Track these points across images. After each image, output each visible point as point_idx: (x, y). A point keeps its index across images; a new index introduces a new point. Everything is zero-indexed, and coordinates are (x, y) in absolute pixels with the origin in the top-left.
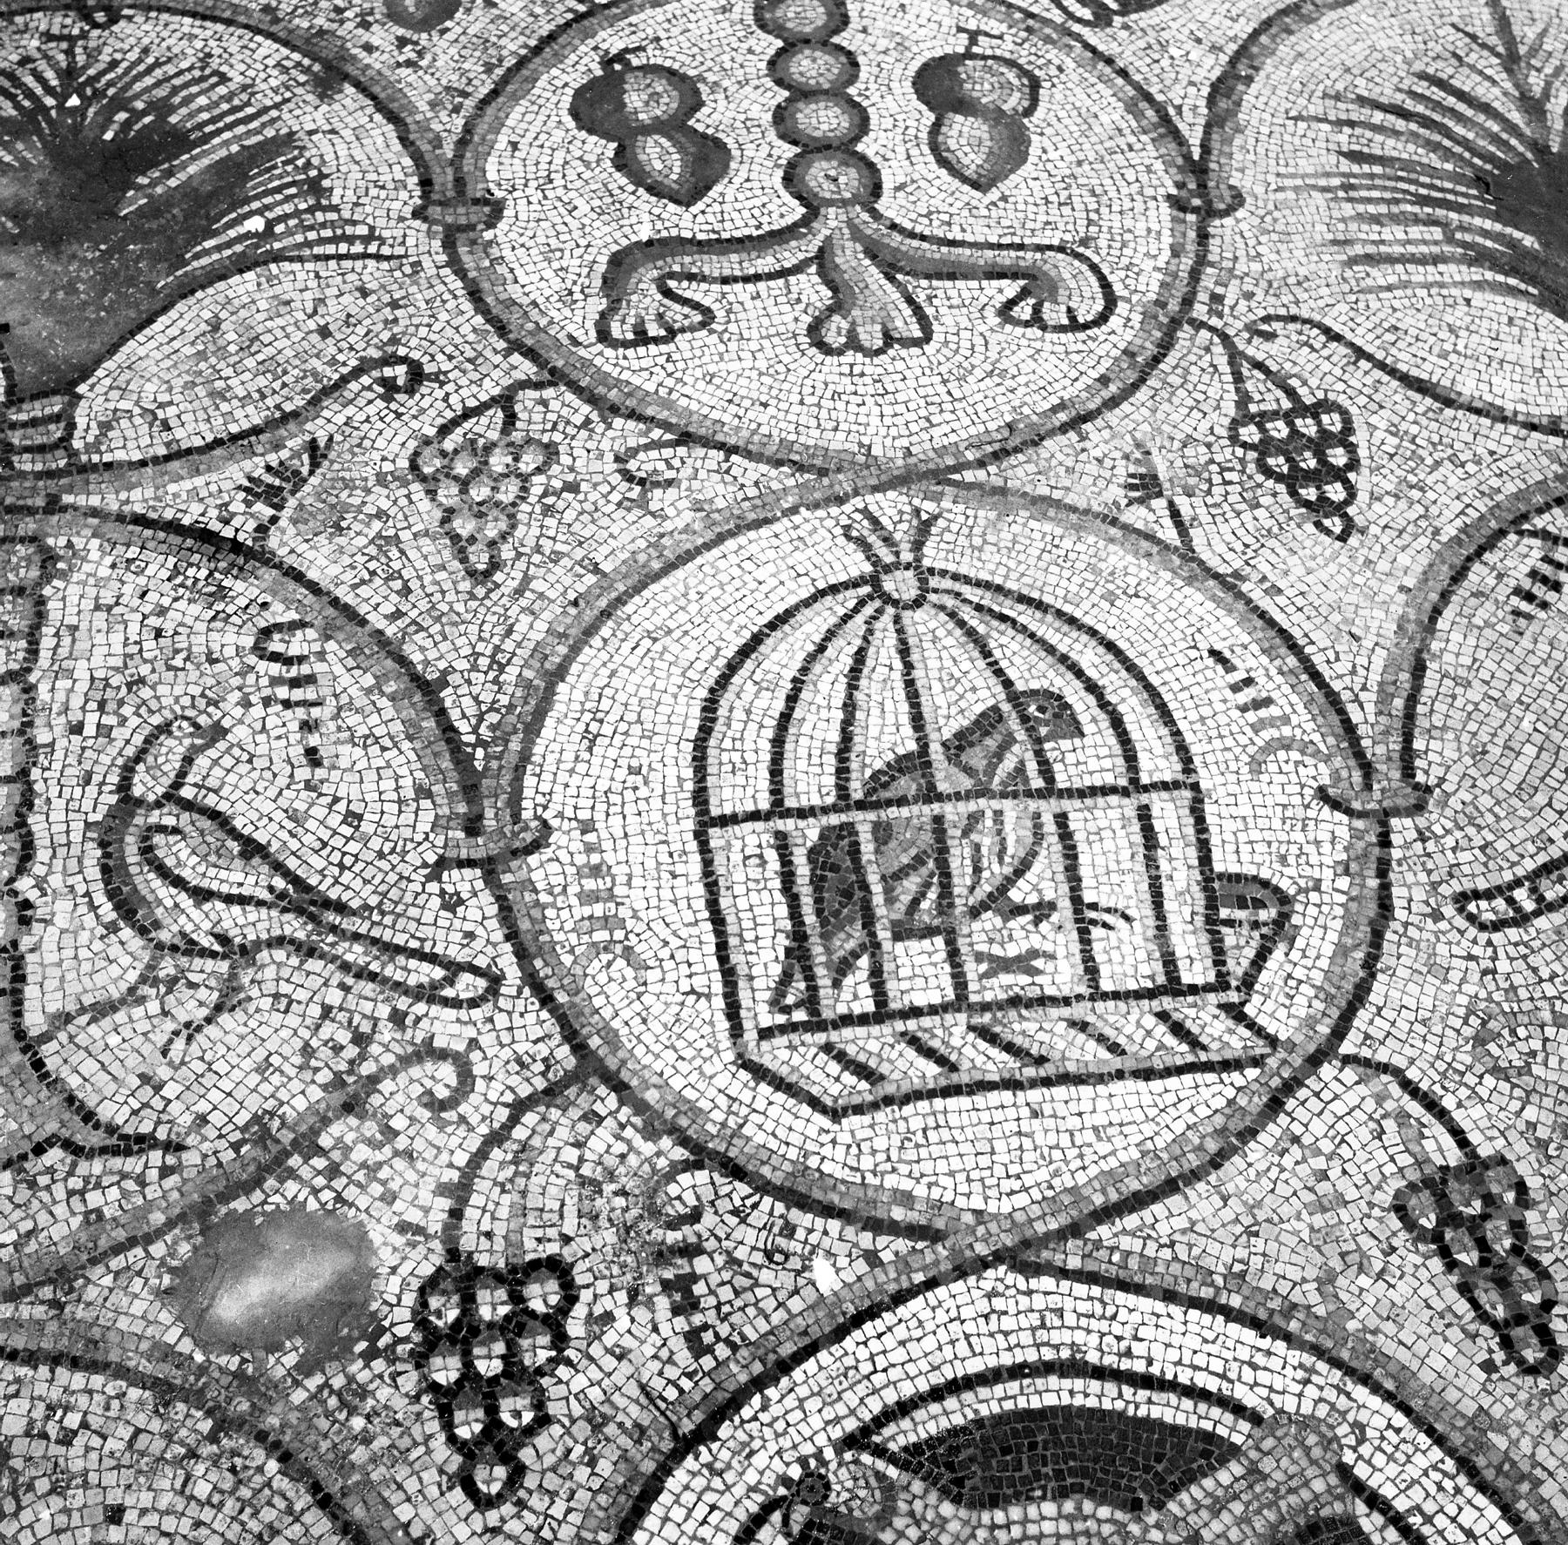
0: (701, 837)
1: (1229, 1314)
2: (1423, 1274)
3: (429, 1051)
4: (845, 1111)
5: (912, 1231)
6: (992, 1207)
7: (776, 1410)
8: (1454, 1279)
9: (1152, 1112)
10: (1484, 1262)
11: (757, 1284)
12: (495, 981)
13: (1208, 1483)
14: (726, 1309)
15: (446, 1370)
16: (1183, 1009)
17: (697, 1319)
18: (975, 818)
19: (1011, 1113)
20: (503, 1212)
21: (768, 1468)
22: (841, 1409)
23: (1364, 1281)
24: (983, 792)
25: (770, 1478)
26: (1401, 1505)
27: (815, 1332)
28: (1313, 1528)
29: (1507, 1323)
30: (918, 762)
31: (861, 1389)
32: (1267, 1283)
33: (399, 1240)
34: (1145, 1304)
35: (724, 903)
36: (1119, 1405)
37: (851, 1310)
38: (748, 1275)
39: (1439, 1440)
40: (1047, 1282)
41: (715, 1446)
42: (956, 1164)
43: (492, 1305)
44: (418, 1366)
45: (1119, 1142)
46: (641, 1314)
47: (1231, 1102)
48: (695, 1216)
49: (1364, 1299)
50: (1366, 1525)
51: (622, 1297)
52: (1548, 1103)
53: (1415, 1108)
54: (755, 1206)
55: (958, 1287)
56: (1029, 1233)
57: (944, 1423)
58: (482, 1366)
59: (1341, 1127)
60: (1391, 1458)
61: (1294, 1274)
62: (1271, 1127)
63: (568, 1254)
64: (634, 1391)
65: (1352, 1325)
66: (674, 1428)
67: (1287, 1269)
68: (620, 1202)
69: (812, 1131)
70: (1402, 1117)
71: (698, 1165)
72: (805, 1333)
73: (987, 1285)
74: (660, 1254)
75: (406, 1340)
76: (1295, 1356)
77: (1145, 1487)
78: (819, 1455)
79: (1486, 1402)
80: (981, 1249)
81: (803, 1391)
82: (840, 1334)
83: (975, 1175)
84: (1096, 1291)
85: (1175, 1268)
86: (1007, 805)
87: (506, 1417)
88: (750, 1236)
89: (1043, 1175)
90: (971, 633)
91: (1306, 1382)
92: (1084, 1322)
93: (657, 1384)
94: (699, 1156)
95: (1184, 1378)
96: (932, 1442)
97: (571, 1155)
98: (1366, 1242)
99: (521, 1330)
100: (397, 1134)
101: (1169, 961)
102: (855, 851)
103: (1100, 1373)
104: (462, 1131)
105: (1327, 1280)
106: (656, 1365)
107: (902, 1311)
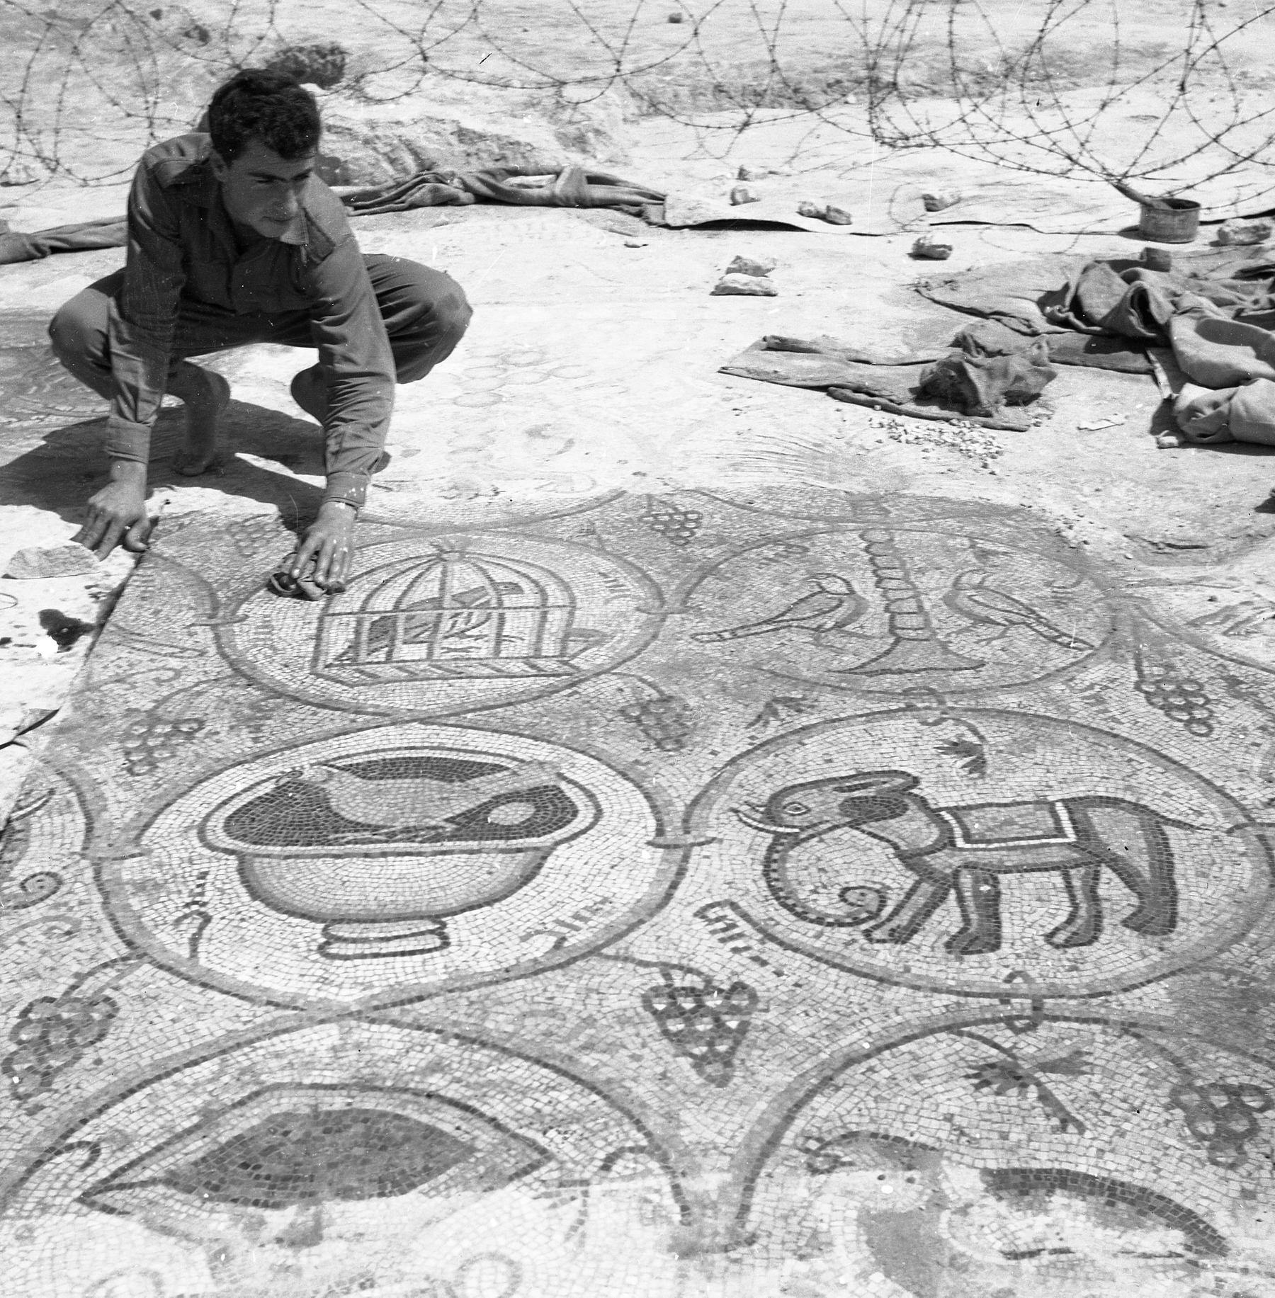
0: (321, 620)
1: (521, 735)
3: (164, 668)
12: (202, 653)
16: (541, 663)
18: (457, 615)
21: (275, 770)
24: (465, 605)
30: (437, 603)
35: (324, 635)
82: (326, 739)
86: (476, 612)
90: (480, 569)
101: (538, 650)
102: (394, 623)
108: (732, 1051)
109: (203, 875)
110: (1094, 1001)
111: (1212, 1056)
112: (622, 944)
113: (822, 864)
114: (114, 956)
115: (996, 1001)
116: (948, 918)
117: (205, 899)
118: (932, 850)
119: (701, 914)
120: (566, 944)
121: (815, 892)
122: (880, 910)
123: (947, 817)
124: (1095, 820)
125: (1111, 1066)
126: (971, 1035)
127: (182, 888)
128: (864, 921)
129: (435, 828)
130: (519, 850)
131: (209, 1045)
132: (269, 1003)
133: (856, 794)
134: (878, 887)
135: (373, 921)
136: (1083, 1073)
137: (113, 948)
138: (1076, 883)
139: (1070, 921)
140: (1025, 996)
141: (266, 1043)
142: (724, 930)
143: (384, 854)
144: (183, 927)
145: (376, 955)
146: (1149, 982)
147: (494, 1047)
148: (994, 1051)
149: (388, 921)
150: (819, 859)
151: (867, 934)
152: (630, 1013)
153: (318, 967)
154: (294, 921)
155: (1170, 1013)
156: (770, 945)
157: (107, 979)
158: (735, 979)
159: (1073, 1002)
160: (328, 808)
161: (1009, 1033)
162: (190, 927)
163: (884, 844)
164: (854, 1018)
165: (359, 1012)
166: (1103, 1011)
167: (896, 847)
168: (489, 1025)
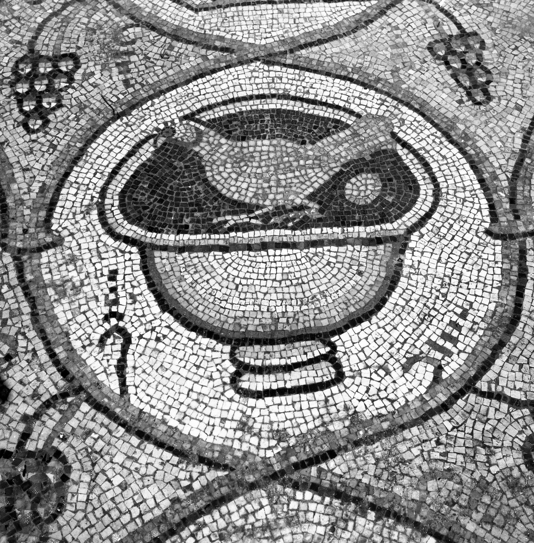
1: (352, 80)
2: (437, 70)
4: (200, 10)
5: (223, 49)
6: (257, 42)
7: (156, 106)
8: (450, 72)
9: (329, 13)
10: (463, 67)
11: (155, 65)
13: (335, 137)
14: (142, 73)
15: (22, 88)
17: (129, 76)
19: (270, 12)
20: (54, 38)
21: (150, 125)
22: (184, 107)
23: (411, 72)
25: (151, 128)
26: (416, 146)
27: (177, 82)
28: (377, 153)
29: (470, 88)
31: (193, 101)
32: (370, 71)
33: (10, 46)
34: (317, 76)
36: (301, 109)
37: (193, 74)
38: (152, 62)
39: (436, 125)
40: (277, 68)
41: (129, 117)
42: (244, 28)
43: (44, 68)
44: (11, 86)
45: (314, 23)
46: (106, 73)
47: (364, 11)
48: (133, 42)
49: (410, 79)
50: (400, 153)
51: (99, 67)
52: (498, 16)
53: (441, 15)
54: (158, 40)
55: (239, 68)
56: (271, 51)
57: (226, 112)
58: (37, 88)
59: (409, 21)
60: (414, 131)
61: (382, 68)
62: (379, 20)
63: (78, 52)
64: (99, 97)
65: (404, 86)
66: (114, 110)
67: (379, 69)
68: (102, 36)
69: (186, 16)
70: (434, 18)
71: (138, 26)
72: (173, 82)
73: (251, 68)
74: (117, 54)
75: (8, 78)
76: (378, 96)
77: (309, 137)
78: (172, 122)
79: (457, 113)
80: (251, 56)
81: (169, 100)
83: (252, 32)
84: (297, 71)
85: (332, 65)
87: (45, 104)
88: (155, 49)
89: (281, 32)
91: (381, 104)
92: (290, 82)
93: (109, 96)
94: (137, 22)
95: (330, 101)
96: (220, 118)
97: (85, 20)
98: (413, 59)
99: (55, 76)
100: (15, 11)
103: (295, 99)
104: (41, 12)
105: (395, 71)
106: (110, 90)
107: (214, 75)
109: (113, 275)
112: (490, 375)
114: (54, 391)
117: (121, 310)
120: (444, 376)
127: (98, 293)
129: (302, 208)
130: (379, 241)
131: (156, 522)
132: (202, 460)
135: (272, 342)
137: (51, 382)
141: (207, 519)
143: (264, 246)
144: (107, 349)
145: (282, 392)
147: (407, 521)
149: (284, 341)
152: (516, 473)
153: (234, 407)
154: (205, 341)
157: (51, 424)
160: (205, 180)
162: (114, 347)
165: (282, 472)
168: (398, 490)
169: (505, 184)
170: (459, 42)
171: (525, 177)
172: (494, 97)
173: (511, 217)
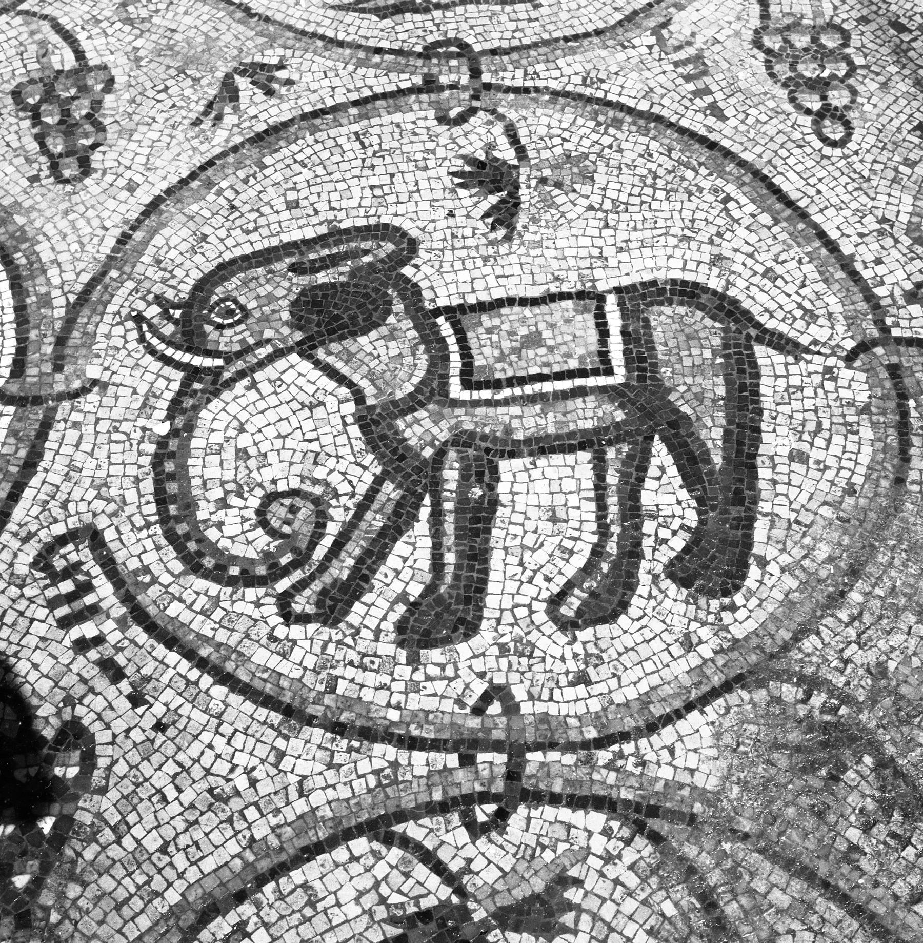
8: (35, 131)
10: (61, 122)
29: (60, 155)
52: (155, 37)
53: (55, 38)
70: (43, 44)
108: (37, 884)
110: (603, 756)
111: (761, 887)
113: (244, 441)
115: (453, 760)
116: (409, 565)
118: (412, 403)
119: (42, 562)
121: (223, 504)
122: (313, 545)
123: (445, 328)
124: (658, 336)
125: (607, 912)
126: (405, 842)
128: (286, 571)
133: (322, 278)
134: (318, 490)
136: (565, 930)
138: (612, 478)
139: (589, 569)
140: (497, 746)
142: (70, 598)
146: (689, 707)
148: (434, 881)
150: (241, 429)
151: (284, 601)
155: (712, 784)
156: (138, 633)
158: (67, 715)
159: (569, 759)
161: (463, 835)
163: (344, 392)
164: (236, 804)
166: (612, 777)
167: (359, 397)
169: (61, 312)
170: (69, 82)
171: (100, 301)
172: (96, 171)
173: (47, 368)
